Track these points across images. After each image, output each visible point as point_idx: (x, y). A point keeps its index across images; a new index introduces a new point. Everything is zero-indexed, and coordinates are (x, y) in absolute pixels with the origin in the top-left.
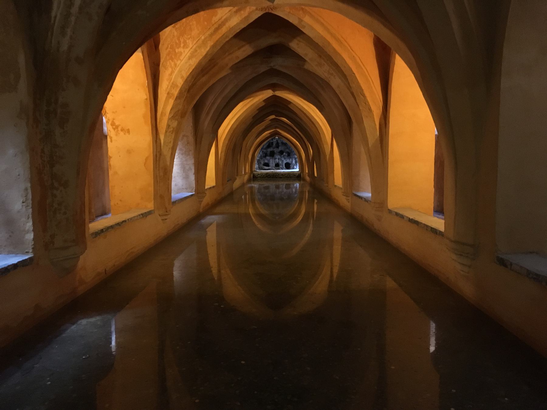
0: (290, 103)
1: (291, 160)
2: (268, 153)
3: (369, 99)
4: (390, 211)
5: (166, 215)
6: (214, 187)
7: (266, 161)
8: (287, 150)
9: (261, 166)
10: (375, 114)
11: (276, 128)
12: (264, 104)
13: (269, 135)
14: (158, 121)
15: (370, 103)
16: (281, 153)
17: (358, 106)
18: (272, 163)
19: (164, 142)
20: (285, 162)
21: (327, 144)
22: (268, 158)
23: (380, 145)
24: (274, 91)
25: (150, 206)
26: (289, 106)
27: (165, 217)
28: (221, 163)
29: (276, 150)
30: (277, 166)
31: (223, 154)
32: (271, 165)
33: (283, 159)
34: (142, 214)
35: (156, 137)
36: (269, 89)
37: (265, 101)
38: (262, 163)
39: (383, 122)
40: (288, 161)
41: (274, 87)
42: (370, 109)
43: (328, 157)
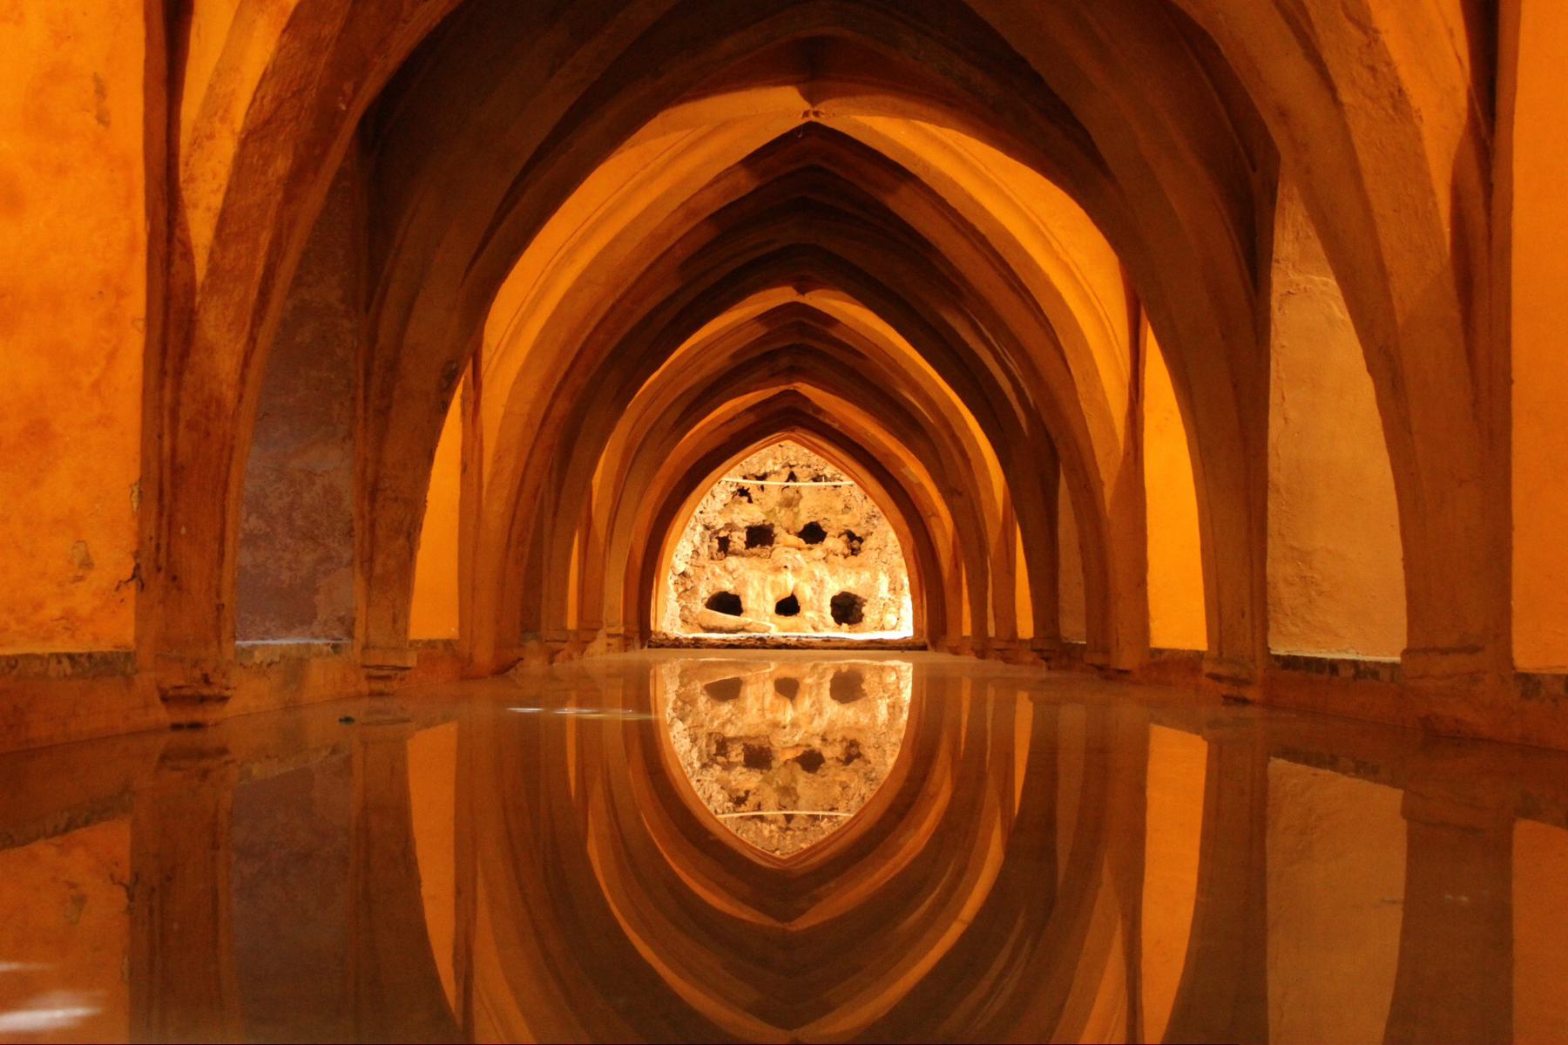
0: (896, 172)
1: (866, 575)
2: (738, 540)
3: (1394, 42)
4: (1530, 683)
5: (203, 699)
6: (448, 643)
7: (728, 586)
8: (847, 521)
9: (699, 607)
10: (1426, 131)
11: (794, 372)
12: (746, 183)
13: (751, 418)
14: (185, 138)
15: (1403, 72)
16: (813, 534)
17: (1332, 89)
18: (758, 586)
19: (213, 271)
20: (834, 587)
21: (1107, 419)
22: (732, 562)
23: (1455, 314)
24: (810, 96)
25: (118, 628)
26: (891, 202)
27: (198, 716)
28: (496, 509)
29: (782, 521)
30: (788, 606)
31: (510, 463)
32: (748, 602)
33: (821, 571)
34: (70, 657)
35: (170, 240)
36: (785, 83)
37: (752, 161)
38: (704, 593)
39: (1473, 180)
40: (849, 582)
41: (813, 68)
42: (1398, 96)
43: (1108, 493)
